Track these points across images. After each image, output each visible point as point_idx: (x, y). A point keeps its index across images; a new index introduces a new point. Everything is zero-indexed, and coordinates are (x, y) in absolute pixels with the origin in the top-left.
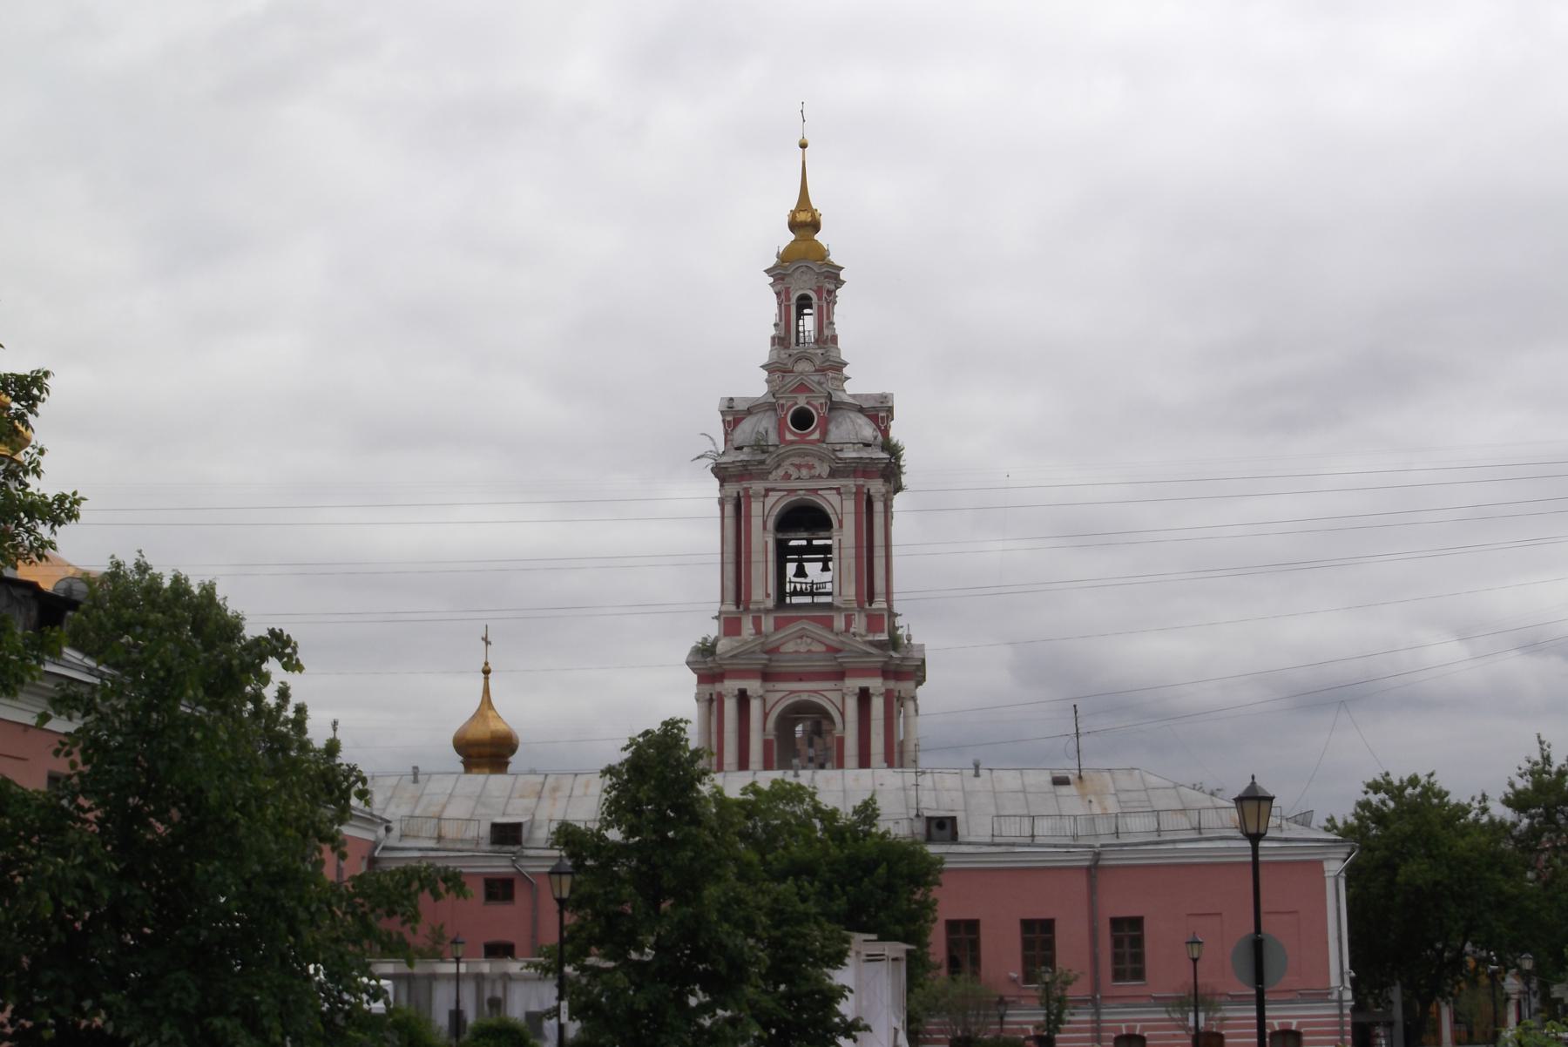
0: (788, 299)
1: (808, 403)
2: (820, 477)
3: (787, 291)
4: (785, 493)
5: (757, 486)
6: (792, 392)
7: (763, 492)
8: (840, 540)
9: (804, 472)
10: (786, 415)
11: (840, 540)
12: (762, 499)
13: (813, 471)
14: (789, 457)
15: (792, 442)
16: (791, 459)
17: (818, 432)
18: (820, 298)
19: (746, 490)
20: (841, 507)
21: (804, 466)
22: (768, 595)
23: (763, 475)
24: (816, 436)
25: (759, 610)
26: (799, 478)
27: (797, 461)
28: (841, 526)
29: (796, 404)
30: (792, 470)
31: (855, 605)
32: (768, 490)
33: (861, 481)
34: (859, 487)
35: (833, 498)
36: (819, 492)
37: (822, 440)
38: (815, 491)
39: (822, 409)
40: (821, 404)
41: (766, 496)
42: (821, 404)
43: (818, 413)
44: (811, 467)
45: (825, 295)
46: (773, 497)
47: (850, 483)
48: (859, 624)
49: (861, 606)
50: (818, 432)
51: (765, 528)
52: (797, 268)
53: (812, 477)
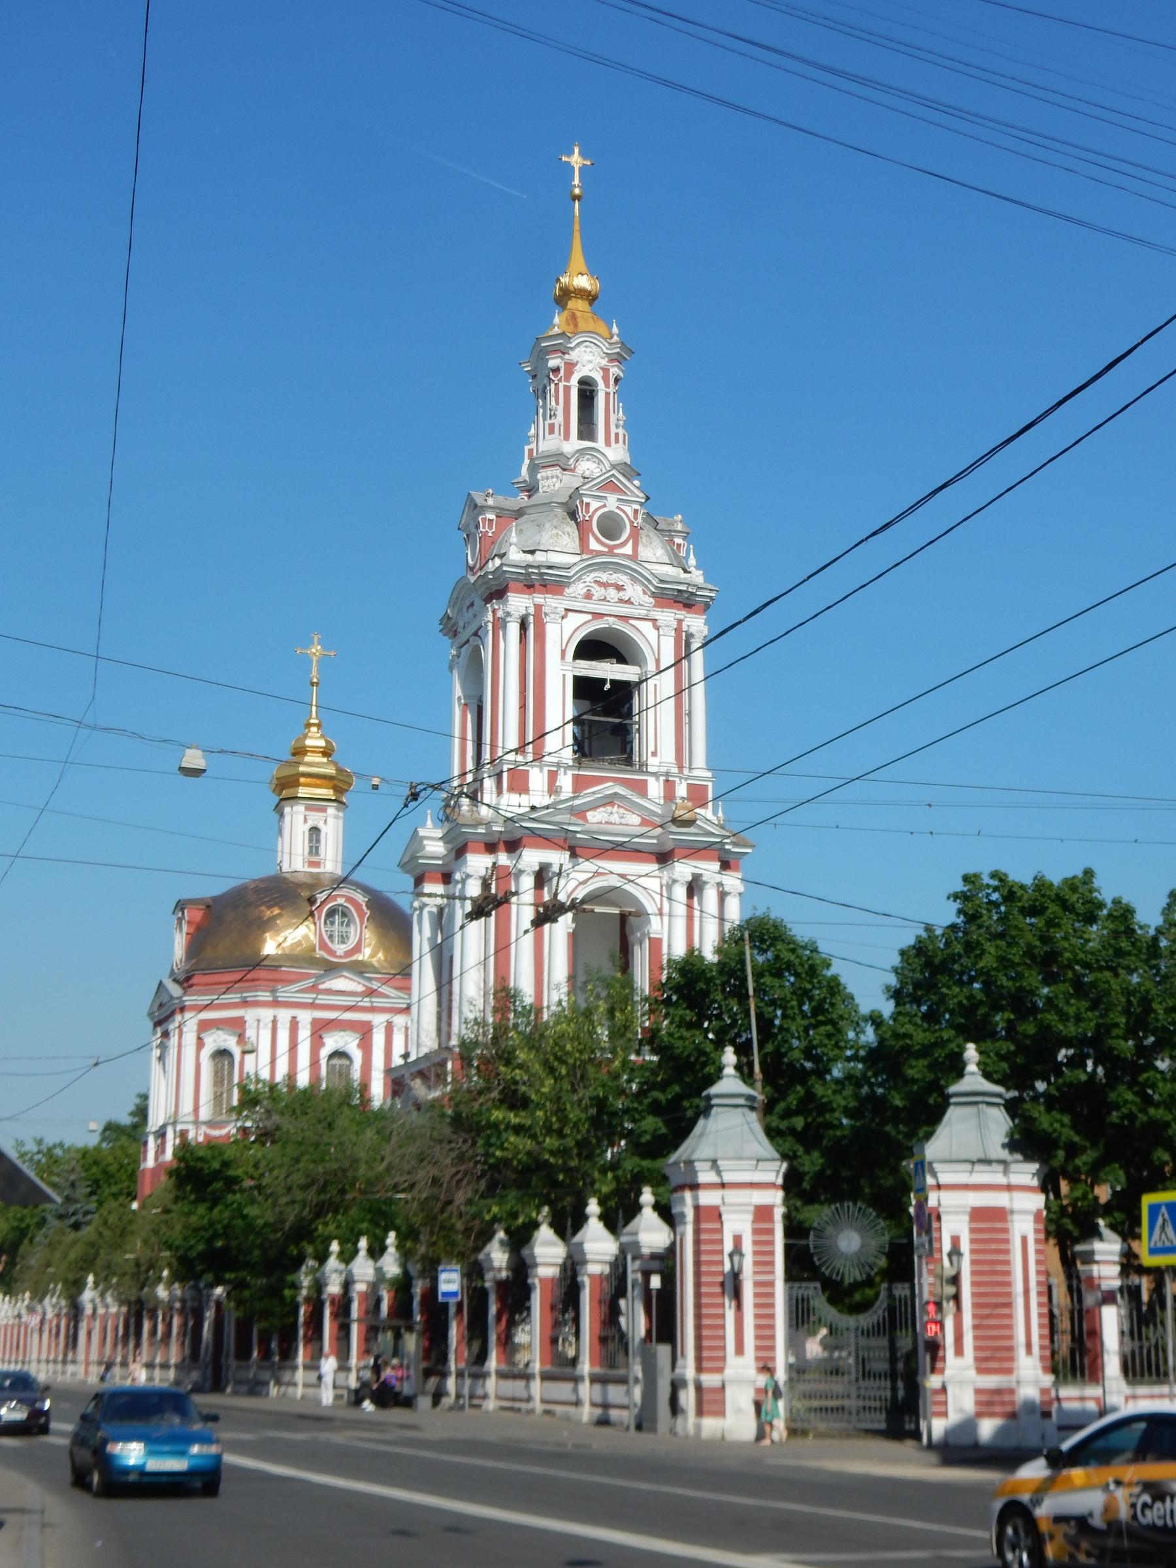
2: (629, 602)
9: (612, 593)
13: (621, 593)
15: (599, 554)
26: (605, 599)
29: (604, 506)
36: (631, 621)
38: (624, 618)
43: (631, 522)
44: (620, 588)
47: (668, 617)
53: (621, 601)
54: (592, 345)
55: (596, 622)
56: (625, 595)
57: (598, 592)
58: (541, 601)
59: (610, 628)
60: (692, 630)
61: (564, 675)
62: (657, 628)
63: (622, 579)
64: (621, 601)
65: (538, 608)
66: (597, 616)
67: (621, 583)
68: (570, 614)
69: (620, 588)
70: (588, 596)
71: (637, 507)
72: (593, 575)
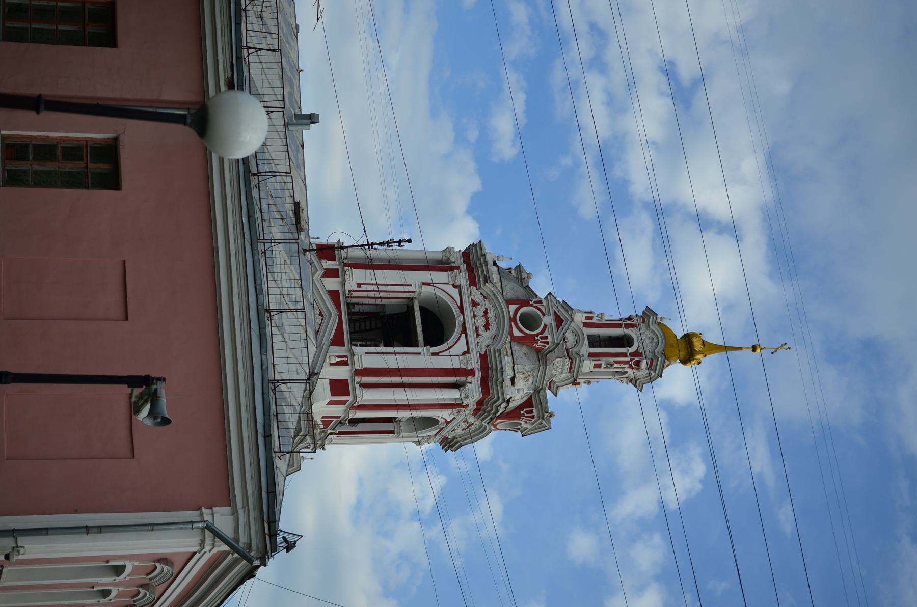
0: (627, 326)
1: (545, 326)
2: (478, 335)
3: (633, 326)
4: (459, 304)
5: (462, 277)
6: (555, 313)
7: (457, 284)
8: (420, 354)
9: (481, 322)
10: (532, 305)
11: (420, 354)
12: (451, 282)
13: (483, 329)
14: (494, 306)
16: (492, 309)
17: (519, 334)
18: (632, 355)
19: (458, 268)
21: (487, 319)
22: (359, 285)
23: (473, 282)
24: (516, 333)
25: (344, 273)
26: (475, 316)
27: (491, 315)
28: (433, 354)
29: (544, 315)
30: (480, 311)
31: (357, 368)
33: (478, 374)
34: (471, 373)
35: (461, 346)
36: (463, 335)
37: (514, 338)
38: (464, 330)
39: (542, 338)
40: (546, 338)
41: (455, 286)
42: (546, 338)
43: (537, 335)
44: (487, 327)
45: (636, 359)
46: (455, 293)
47: (474, 362)
48: (342, 373)
49: (358, 373)
50: (519, 334)
51: (424, 284)
52: (657, 335)
53: (477, 328)
54: (655, 340)
56: (482, 331)
57: (480, 311)
58: (462, 267)
59: (455, 319)
60: (469, 386)
61: (411, 285)
62: (464, 353)
63: (493, 328)
64: (477, 328)
65: (458, 268)
66: (461, 308)
67: (490, 327)
68: (457, 290)
69: (487, 327)
70: (474, 304)
71: (550, 339)
72: (491, 306)
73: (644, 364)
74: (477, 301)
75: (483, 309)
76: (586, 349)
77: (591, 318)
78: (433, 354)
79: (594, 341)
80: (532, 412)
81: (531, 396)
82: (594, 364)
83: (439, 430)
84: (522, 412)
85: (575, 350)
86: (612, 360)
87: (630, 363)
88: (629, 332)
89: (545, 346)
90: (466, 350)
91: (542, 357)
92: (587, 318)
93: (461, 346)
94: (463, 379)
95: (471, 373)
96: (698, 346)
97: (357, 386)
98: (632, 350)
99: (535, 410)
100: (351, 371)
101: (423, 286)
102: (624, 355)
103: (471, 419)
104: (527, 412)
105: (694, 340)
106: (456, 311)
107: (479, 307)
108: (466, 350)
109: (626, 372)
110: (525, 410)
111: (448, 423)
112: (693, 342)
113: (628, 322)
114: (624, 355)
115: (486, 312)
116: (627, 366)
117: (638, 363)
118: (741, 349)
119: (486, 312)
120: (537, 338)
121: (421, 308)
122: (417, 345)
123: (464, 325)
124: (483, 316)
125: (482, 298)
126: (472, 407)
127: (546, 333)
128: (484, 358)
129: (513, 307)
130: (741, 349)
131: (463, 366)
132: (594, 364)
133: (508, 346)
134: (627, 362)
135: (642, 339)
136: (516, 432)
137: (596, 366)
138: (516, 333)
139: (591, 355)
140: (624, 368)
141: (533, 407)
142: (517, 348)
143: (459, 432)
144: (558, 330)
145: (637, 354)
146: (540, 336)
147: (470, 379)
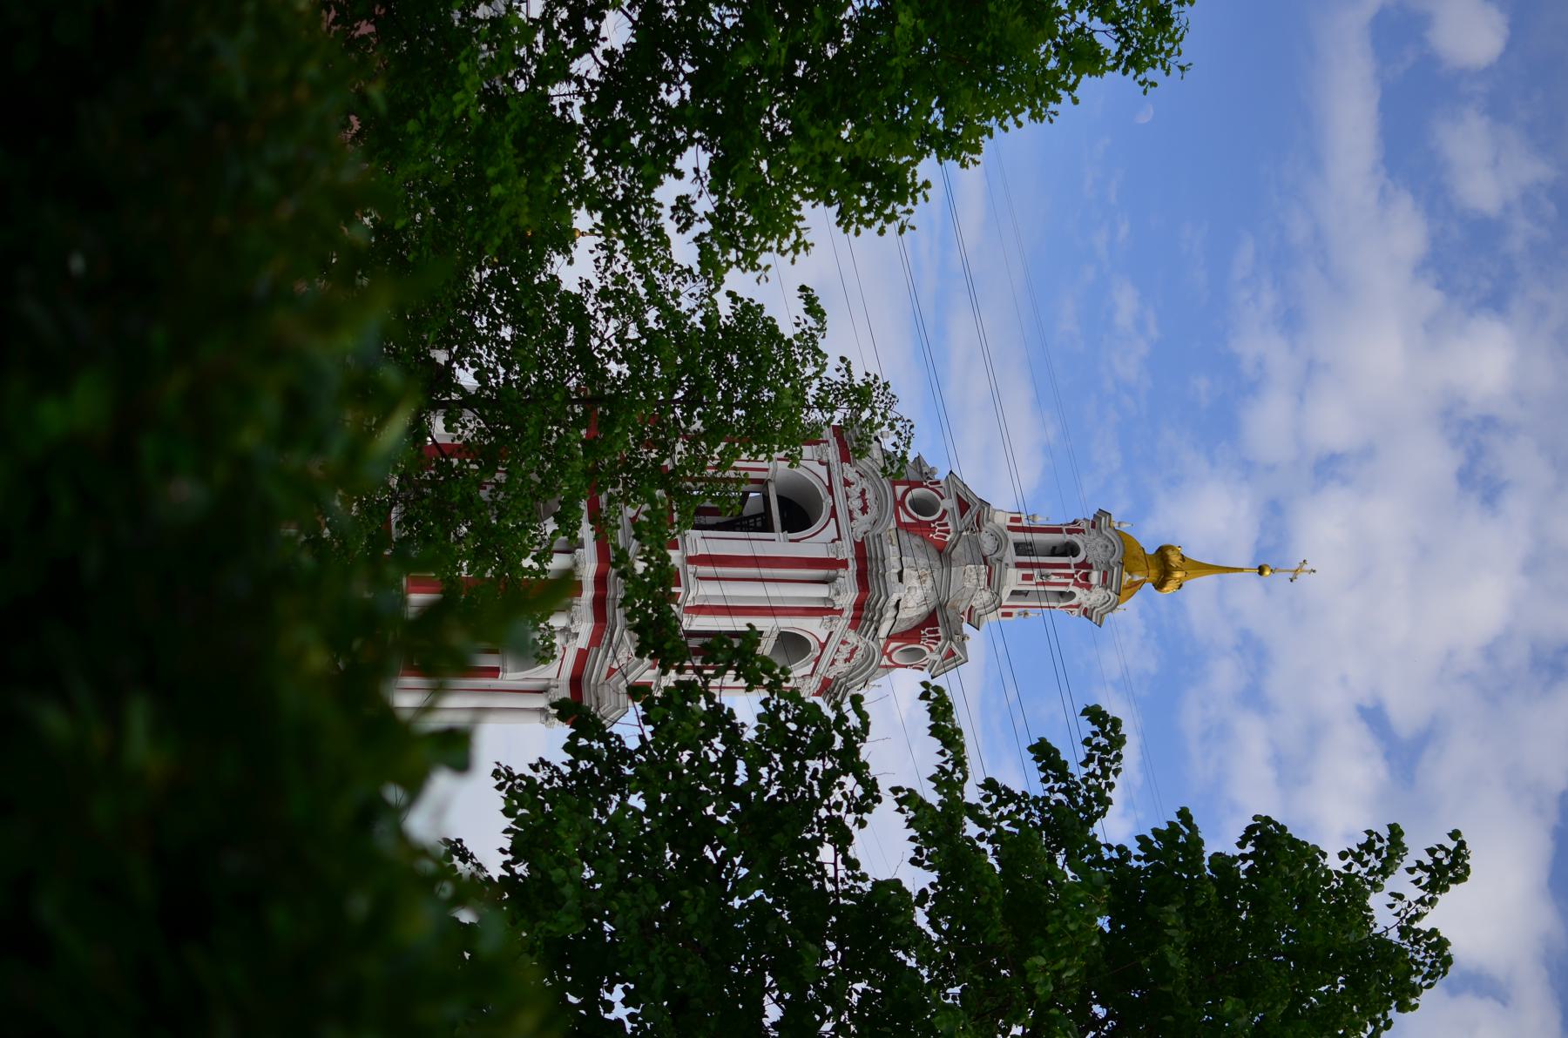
0: (1070, 532)
1: (945, 512)
2: (852, 519)
3: (1078, 531)
4: (827, 484)
5: (832, 452)
6: (959, 497)
8: (774, 540)
9: (856, 504)
10: (927, 487)
11: (774, 540)
12: (816, 458)
13: (860, 512)
16: (872, 490)
18: (1077, 566)
20: (814, 544)
21: (864, 501)
23: (845, 458)
26: (848, 497)
27: (869, 496)
28: (791, 541)
29: (942, 498)
30: (855, 491)
31: (691, 553)
32: (827, 464)
33: (853, 566)
34: (844, 564)
35: (831, 531)
36: (833, 520)
37: (900, 525)
38: (834, 514)
39: (939, 525)
40: (946, 525)
41: (821, 463)
42: (946, 525)
43: (934, 522)
44: (864, 510)
47: (846, 551)
49: (692, 560)
52: (1112, 542)
53: (851, 512)
55: (826, 490)
56: (857, 514)
57: (855, 491)
58: (831, 441)
59: (822, 501)
60: (840, 580)
62: (833, 541)
63: (873, 512)
64: (851, 512)
65: (827, 442)
66: (830, 489)
67: (869, 510)
68: (825, 467)
69: (864, 510)
70: (847, 483)
71: (951, 527)
72: (870, 486)
73: (1095, 577)
74: (851, 479)
75: (859, 489)
76: (1010, 555)
77: (1019, 520)
78: (791, 541)
79: (1021, 548)
80: (936, 631)
81: (935, 610)
82: (1023, 575)
83: (814, 663)
84: (922, 632)
85: (997, 556)
86: (1050, 571)
87: (1075, 576)
88: (1074, 538)
89: (945, 537)
90: (837, 537)
91: (943, 553)
92: (1013, 520)
93: (831, 531)
94: (832, 572)
95: (844, 564)
96: (1174, 559)
97: (691, 578)
98: (1079, 559)
99: (940, 630)
100: (682, 557)
101: (778, 462)
102: (1067, 566)
103: (852, 637)
104: (929, 632)
105: (1170, 553)
106: (823, 492)
107: (853, 487)
108: (837, 537)
109: (1072, 595)
110: (927, 629)
111: (823, 646)
112: (1167, 556)
113: (1071, 527)
114: (1067, 566)
115: (863, 492)
116: (1071, 581)
117: (1086, 577)
118: (1241, 570)
119: (863, 492)
120: (932, 525)
121: (780, 498)
122: (772, 530)
123: (834, 509)
124: (859, 497)
125: (857, 476)
126: (848, 613)
127: (946, 520)
128: (860, 548)
129: (900, 489)
130: (1241, 570)
131: (832, 556)
132: (1023, 575)
133: (893, 533)
134: (1072, 576)
135: (1090, 547)
136: (922, 669)
137: (1025, 577)
138: (905, 518)
139: (1019, 565)
140: (1067, 584)
141: (938, 625)
142: (904, 537)
143: (841, 667)
144: (962, 517)
145: (1084, 565)
146: (937, 523)
147: (841, 572)
